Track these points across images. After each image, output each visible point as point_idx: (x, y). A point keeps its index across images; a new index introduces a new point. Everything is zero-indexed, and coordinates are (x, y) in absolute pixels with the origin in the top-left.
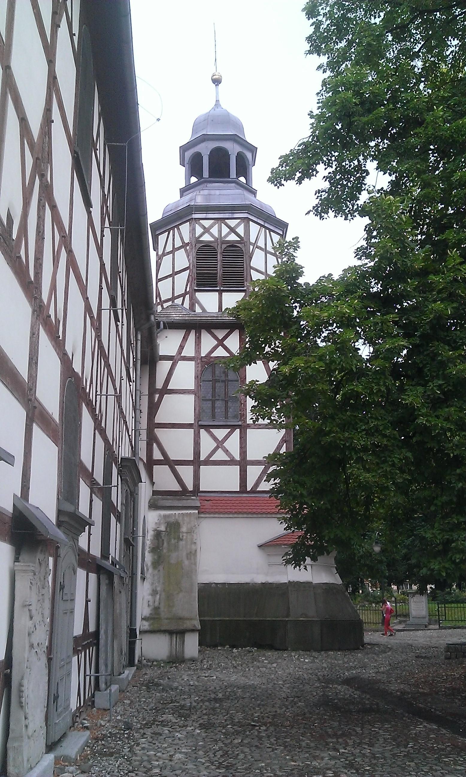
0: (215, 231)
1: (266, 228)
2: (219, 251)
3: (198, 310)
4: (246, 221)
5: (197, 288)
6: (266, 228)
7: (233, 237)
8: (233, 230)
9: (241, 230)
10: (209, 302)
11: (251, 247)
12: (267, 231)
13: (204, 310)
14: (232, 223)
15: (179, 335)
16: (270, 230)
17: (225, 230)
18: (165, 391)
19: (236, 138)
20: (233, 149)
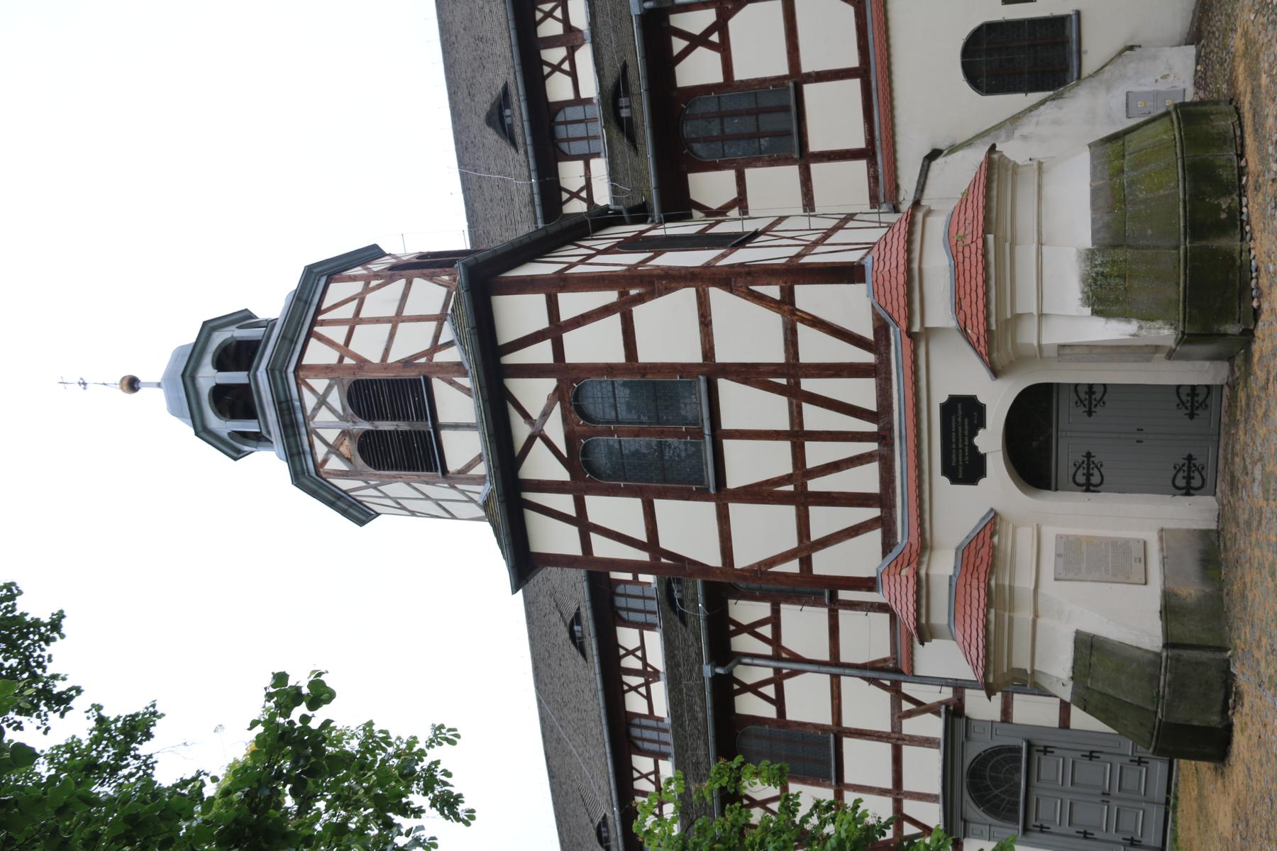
1: (314, 322)
2: (366, 426)
4: (301, 373)
5: (440, 473)
6: (314, 322)
7: (335, 399)
8: (322, 401)
9: (320, 384)
10: (463, 447)
11: (347, 361)
12: (320, 318)
14: (310, 401)
15: (535, 521)
16: (318, 311)
17: (324, 415)
18: (651, 543)
19: (188, 373)
20: (209, 377)
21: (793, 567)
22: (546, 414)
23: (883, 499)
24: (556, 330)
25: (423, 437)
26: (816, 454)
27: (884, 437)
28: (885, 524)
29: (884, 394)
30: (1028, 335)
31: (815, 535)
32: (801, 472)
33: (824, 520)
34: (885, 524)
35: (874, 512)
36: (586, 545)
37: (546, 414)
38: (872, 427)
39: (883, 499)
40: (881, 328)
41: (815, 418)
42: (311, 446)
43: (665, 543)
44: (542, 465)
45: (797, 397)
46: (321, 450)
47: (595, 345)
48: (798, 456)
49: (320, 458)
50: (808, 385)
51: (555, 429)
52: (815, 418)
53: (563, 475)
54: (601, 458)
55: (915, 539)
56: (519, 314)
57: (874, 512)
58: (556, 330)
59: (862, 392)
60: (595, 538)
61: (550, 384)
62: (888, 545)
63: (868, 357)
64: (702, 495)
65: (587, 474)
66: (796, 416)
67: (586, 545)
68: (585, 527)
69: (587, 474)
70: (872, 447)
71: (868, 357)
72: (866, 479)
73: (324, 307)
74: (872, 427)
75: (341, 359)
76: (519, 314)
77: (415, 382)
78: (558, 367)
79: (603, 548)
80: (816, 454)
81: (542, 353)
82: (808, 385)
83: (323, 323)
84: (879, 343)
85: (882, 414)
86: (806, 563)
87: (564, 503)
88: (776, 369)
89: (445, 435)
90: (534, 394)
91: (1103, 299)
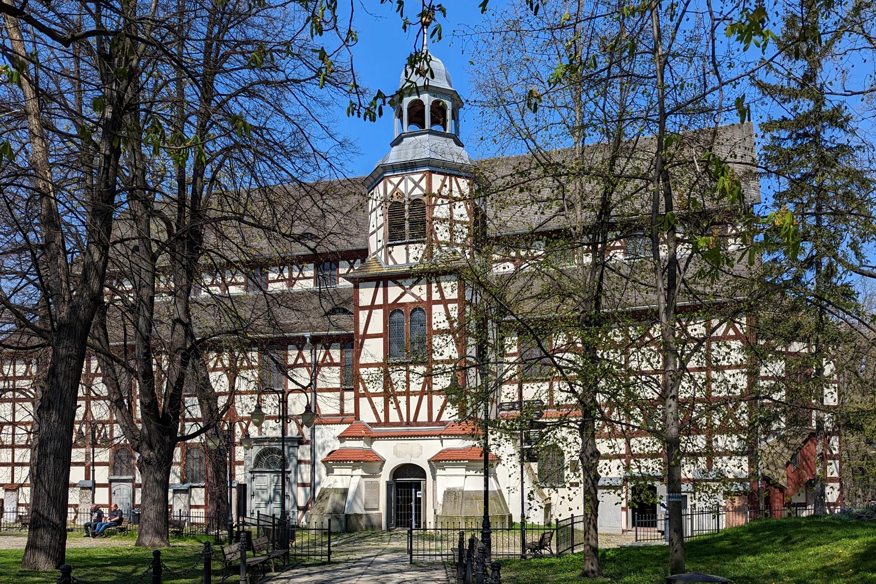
0: (402, 187)
1: (450, 175)
3: (391, 263)
7: (417, 192)
13: (395, 263)
14: (417, 177)
17: (411, 185)
18: (366, 336)
21: (361, 390)
22: (413, 295)
23: (387, 423)
24: (444, 302)
25: (402, 237)
26: (402, 399)
27: (408, 424)
28: (379, 424)
29: (423, 424)
30: (439, 472)
31: (374, 399)
32: (396, 395)
33: (379, 402)
34: (379, 424)
35: (383, 420)
36: (364, 308)
37: (413, 295)
38: (411, 420)
39: (387, 423)
40: (444, 424)
41: (414, 400)
42: (397, 176)
43: (367, 341)
44: (394, 292)
45: (422, 393)
46: (396, 180)
47: (439, 317)
48: (400, 394)
49: (392, 179)
50: (425, 398)
51: (408, 299)
52: (414, 400)
53: (390, 301)
54: (396, 317)
55: (374, 435)
56: (450, 289)
57: (383, 420)
58: (444, 302)
59: (423, 417)
60: (367, 312)
61: (425, 299)
62: (371, 424)
63: (434, 419)
64: (386, 357)
65: (392, 310)
66: (415, 393)
67: (364, 308)
68: (372, 307)
69: (392, 310)
70: (405, 420)
71: (434, 419)
72: (394, 417)
73: (458, 179)
74: (411, 420)
75: (434, 195)
76: (450, 289)
77: (423, 234)
78: (430, 302)
79: (363, 315)
80: (402, 399)
81: (436, 296)
82: (425, 398)
83: (451, 181)
84: (438, 422)
85: (416, 423)
86: (363, 395)
87: (379, 301)
88: (430, 388)
89: (404, 247)
90: (420, 291)
91: (448, 493)
